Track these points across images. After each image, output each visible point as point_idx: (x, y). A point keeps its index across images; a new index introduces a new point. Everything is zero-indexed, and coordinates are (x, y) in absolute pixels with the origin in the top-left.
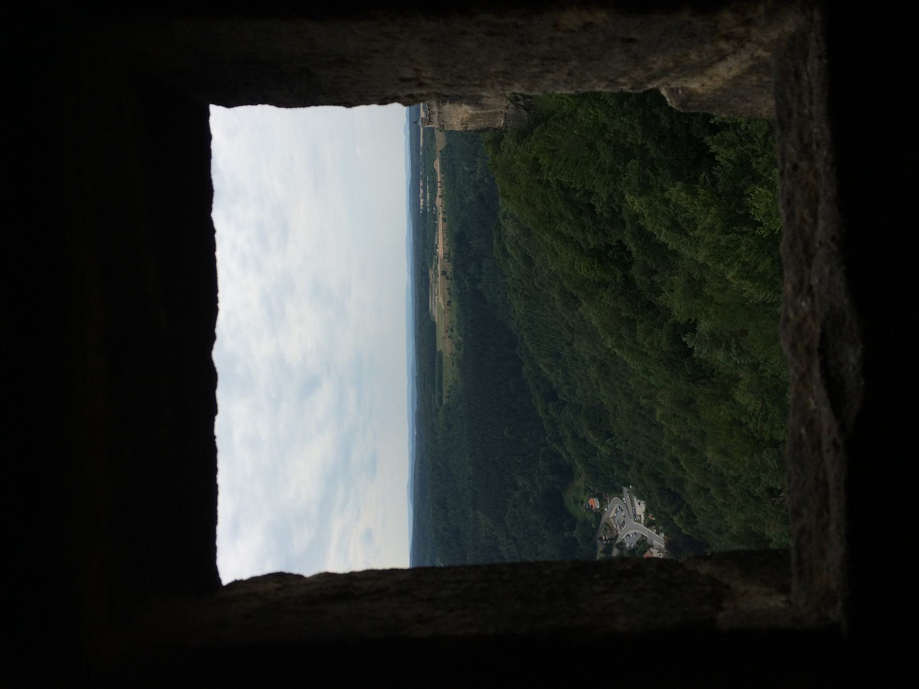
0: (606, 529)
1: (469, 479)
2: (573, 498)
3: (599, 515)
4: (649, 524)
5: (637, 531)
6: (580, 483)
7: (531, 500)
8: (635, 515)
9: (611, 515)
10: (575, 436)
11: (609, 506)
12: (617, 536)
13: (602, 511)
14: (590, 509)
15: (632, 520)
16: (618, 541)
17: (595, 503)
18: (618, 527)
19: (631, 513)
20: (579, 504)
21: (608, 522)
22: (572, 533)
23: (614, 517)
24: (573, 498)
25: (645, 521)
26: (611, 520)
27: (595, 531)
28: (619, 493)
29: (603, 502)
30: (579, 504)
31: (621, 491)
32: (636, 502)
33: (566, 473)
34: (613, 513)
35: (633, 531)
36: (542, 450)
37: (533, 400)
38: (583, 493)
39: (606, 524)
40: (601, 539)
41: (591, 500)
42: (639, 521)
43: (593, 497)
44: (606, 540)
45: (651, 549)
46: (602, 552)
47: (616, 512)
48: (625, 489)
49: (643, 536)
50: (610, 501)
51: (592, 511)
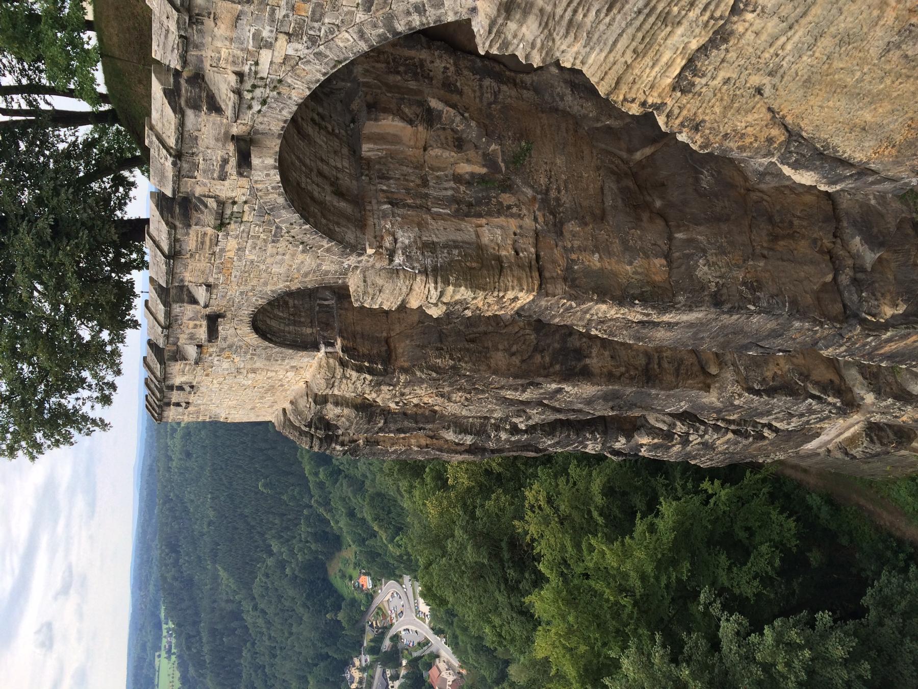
0: (378, 613)
1: (209, 525)
2: (340, 570)
3: (370, 597)
4: (438, 632)
5: (418, 630)
6: (350, 552)
7: (288, 571)
8: (418, 612)
9: (386, 599)
10: (351, 514)
11: (384, 588)
12: (392, 625)
13: (374, 592)
14: (360, 588)
15: (414, 615)
16: (392, 632)
17: (367, 582)
18: (394, 615)
19: (413, 606)
20: (347, 581)
21: (381, 606)
22: (336, 615)
23: (388, 601)
24: (340, 570)
25: (430, 622)
26: (386, 604)
27: (364, 614)
28: (398, 578)
29: (376, 582)
30: (347, 581)
31: (401, 577)
32: (421, 601)
33: (334, 542)
34: (389, 596)
35: (414, 628)
36: (305, 512)
37: (298, 454)
38: (352, 566)
39: (380, 609)
40: (371, 626)
41: (363, 577)
42: (423, 620)
43: (365, 574)
44: (377, 627)
45: (437, 660)
46: (371, 641)
47: (392, 596)
48: (407, 578)
49: (426, 638)
50: (386, 583)
51: (362, 591)
